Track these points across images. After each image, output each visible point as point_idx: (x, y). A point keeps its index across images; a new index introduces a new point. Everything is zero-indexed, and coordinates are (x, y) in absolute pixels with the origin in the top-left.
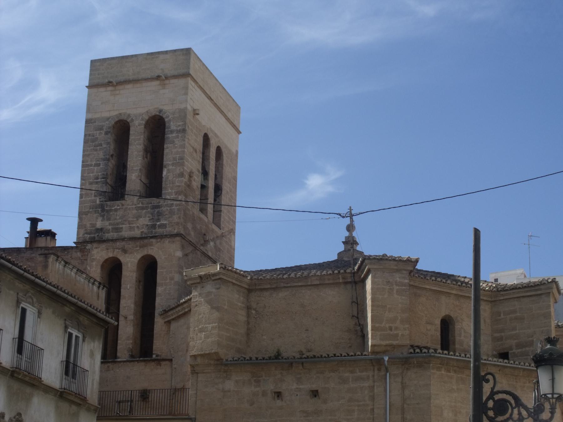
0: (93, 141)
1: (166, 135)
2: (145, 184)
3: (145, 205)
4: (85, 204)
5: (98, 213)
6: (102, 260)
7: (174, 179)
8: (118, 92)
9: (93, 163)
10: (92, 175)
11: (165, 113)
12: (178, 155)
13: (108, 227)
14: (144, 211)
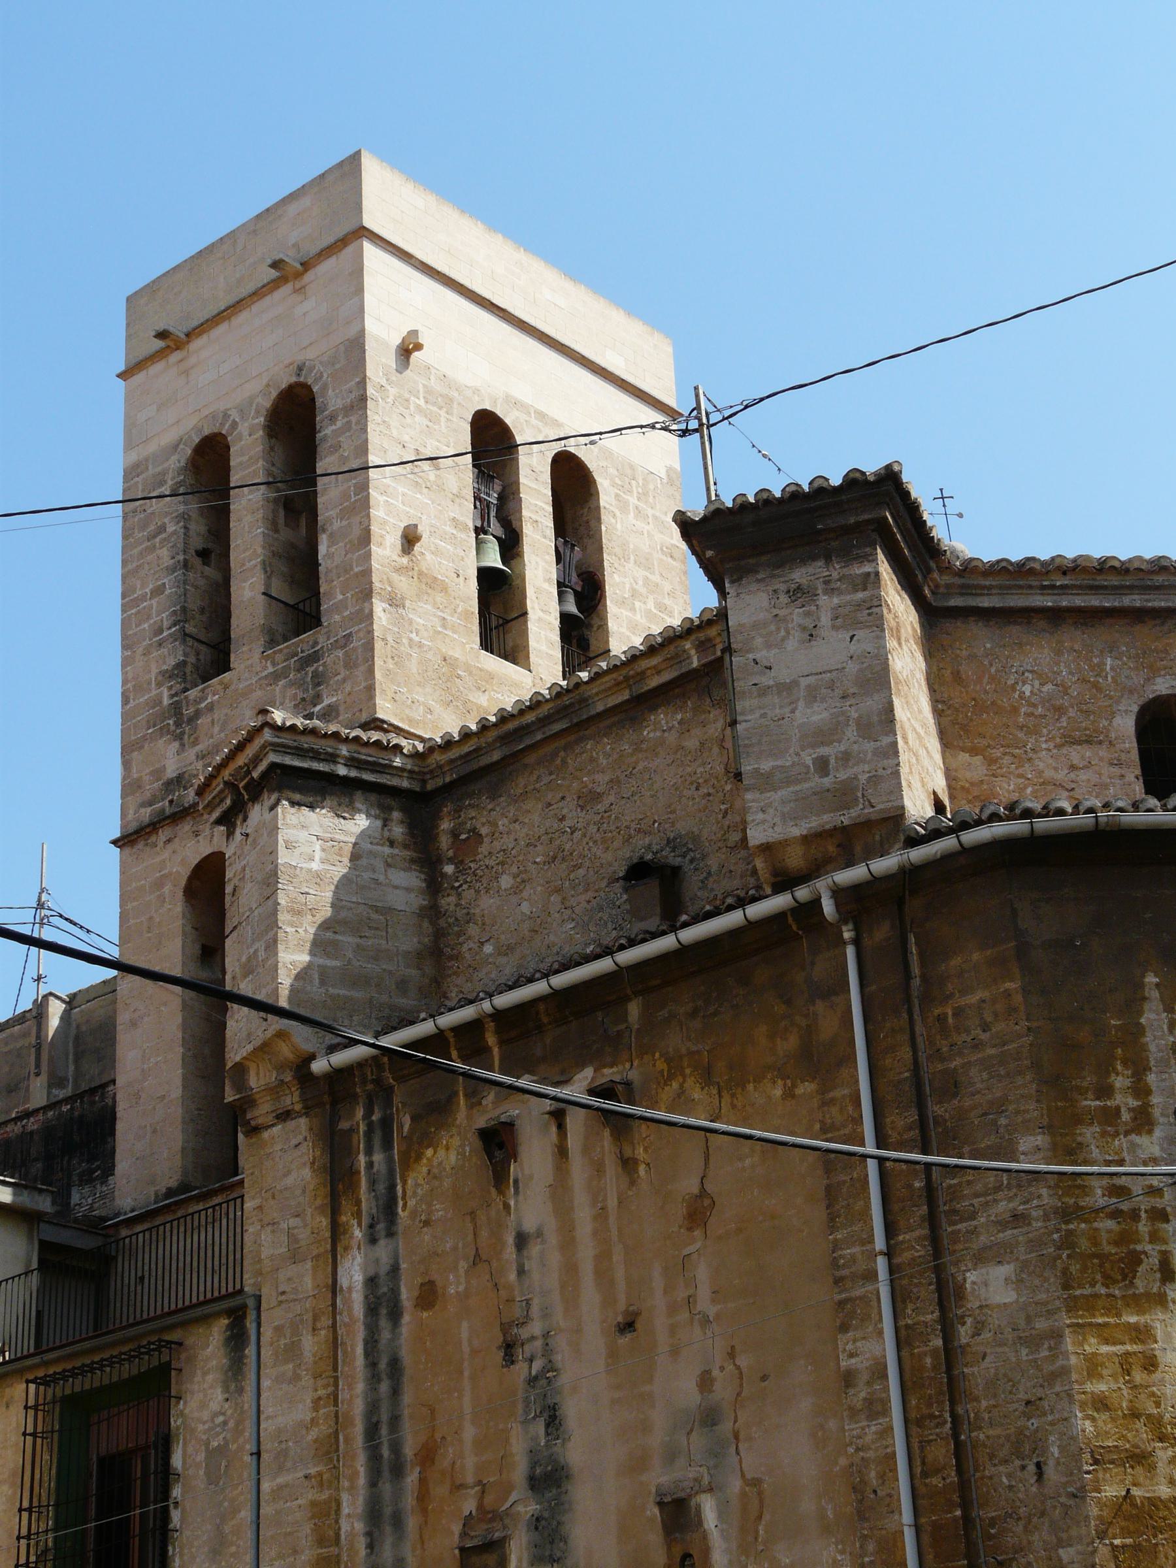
0: (144, 526)
1: (319, 432)
2: (292, 606)
3: (280, 666)
4: (134, 718)
5: (168, 732)
6: (185, 872)
7: (349, 556)
8: (193, 360)
9: (147, 590)
10: (146, 626)
11: (312, 369)
12: (354, 482)
13: (193, 767)
14: (280, 683)
